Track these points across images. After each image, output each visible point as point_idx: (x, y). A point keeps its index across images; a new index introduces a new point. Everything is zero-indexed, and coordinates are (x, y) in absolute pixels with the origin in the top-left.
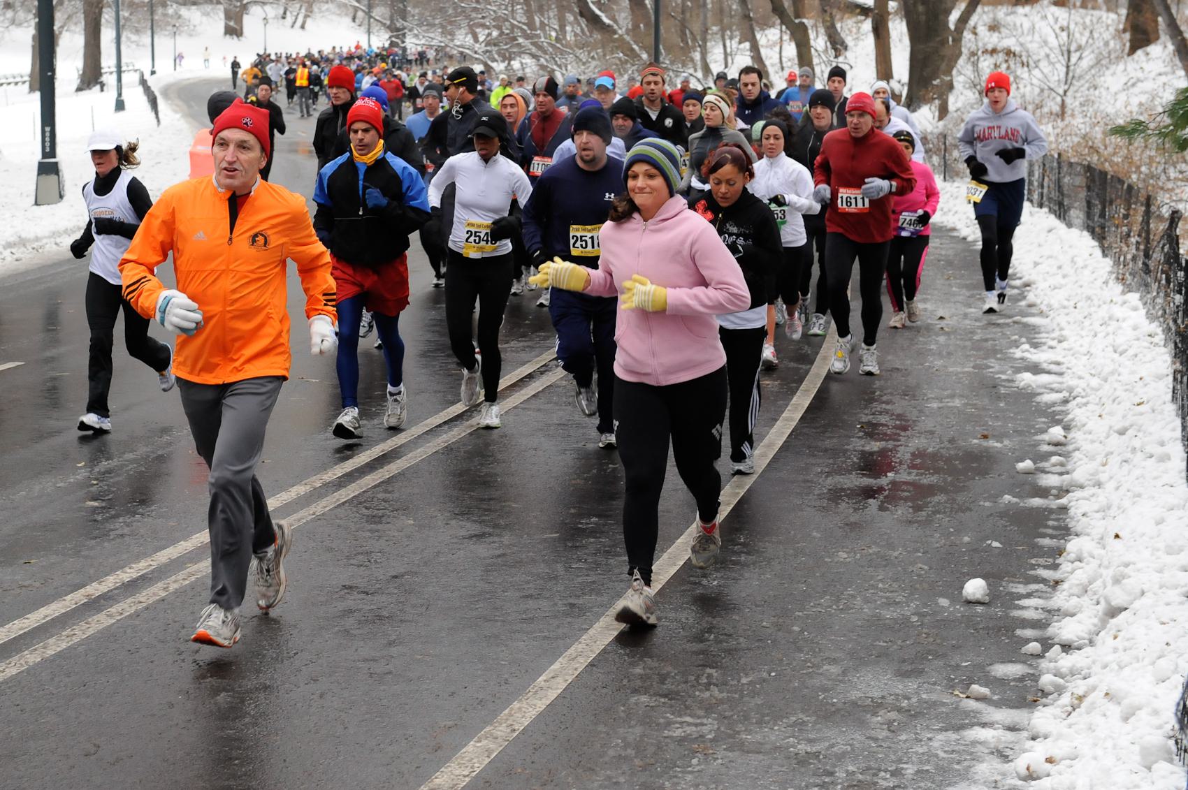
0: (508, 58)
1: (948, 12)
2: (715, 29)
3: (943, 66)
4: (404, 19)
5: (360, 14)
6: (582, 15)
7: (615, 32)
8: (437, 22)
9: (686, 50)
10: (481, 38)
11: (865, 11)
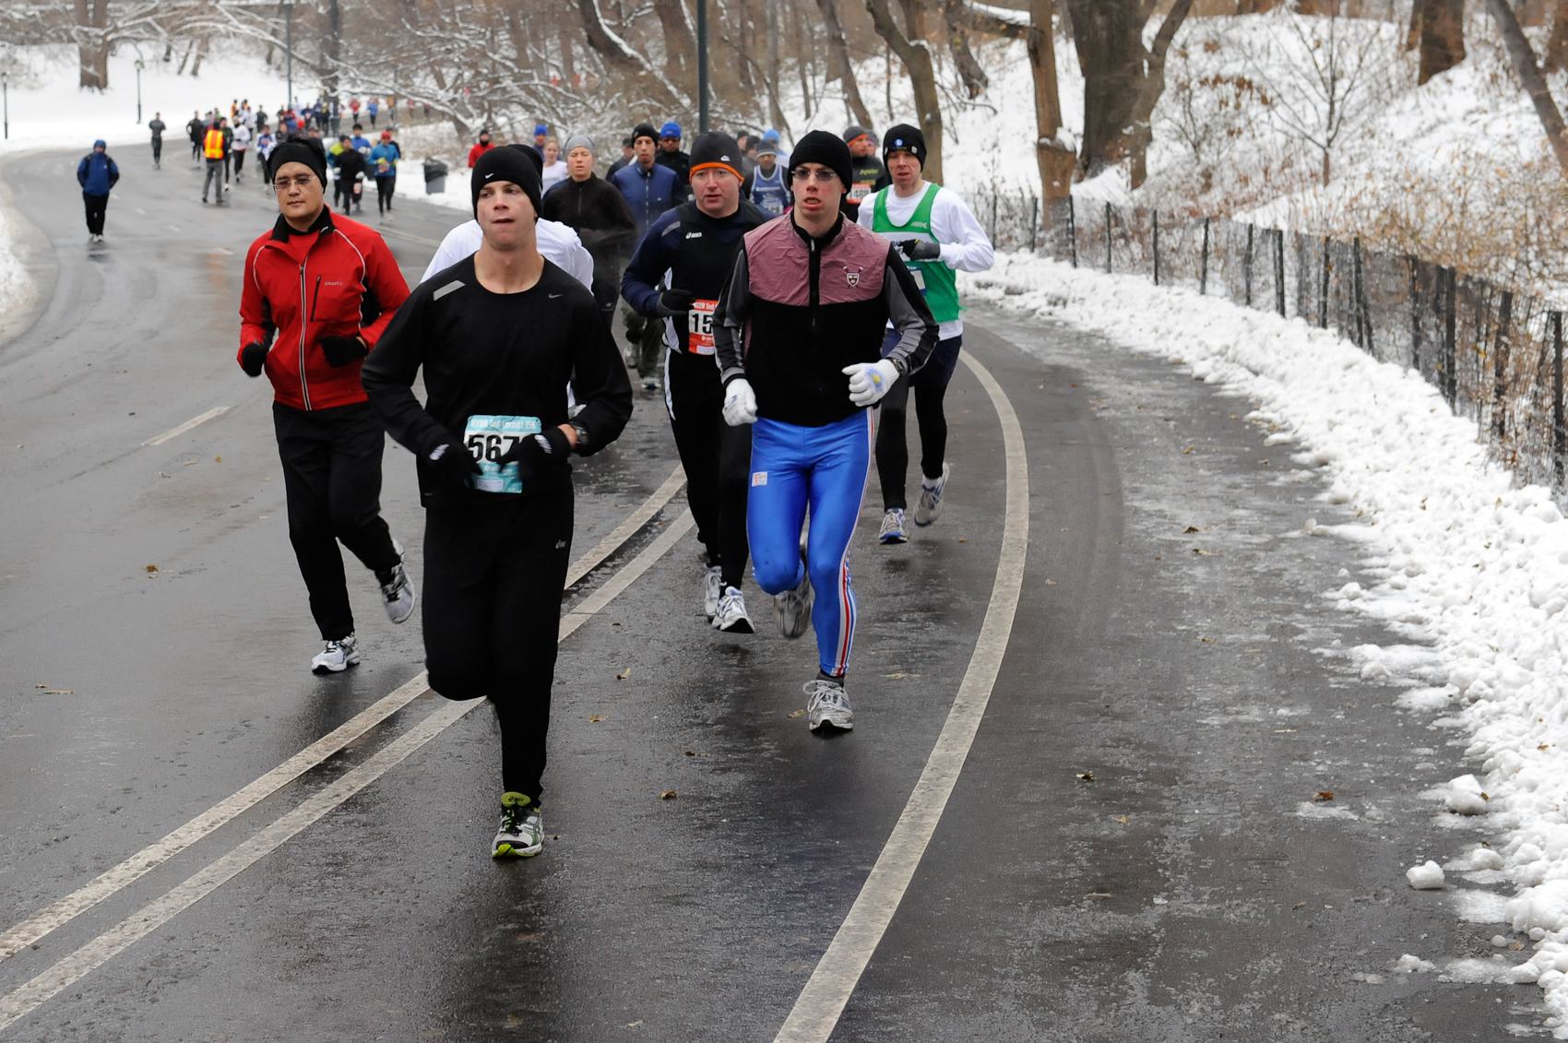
0: (487, 108)
1: (1141, 24)
2: (790, 61)
3: (1137, 107)
4: (334, 55)
5: (277, 53)
6: (591, 42)
7: (641, 67)
8: (382, 59)
9: (749, 92)
10: (449, 81)
11: (1013, 30)
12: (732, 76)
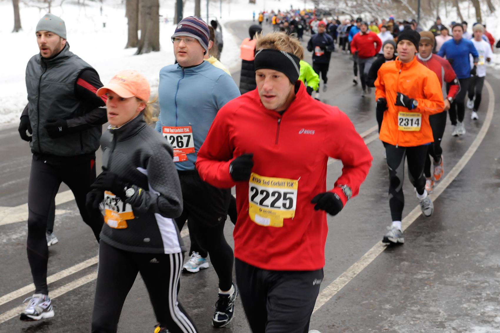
12: (426, 6)
